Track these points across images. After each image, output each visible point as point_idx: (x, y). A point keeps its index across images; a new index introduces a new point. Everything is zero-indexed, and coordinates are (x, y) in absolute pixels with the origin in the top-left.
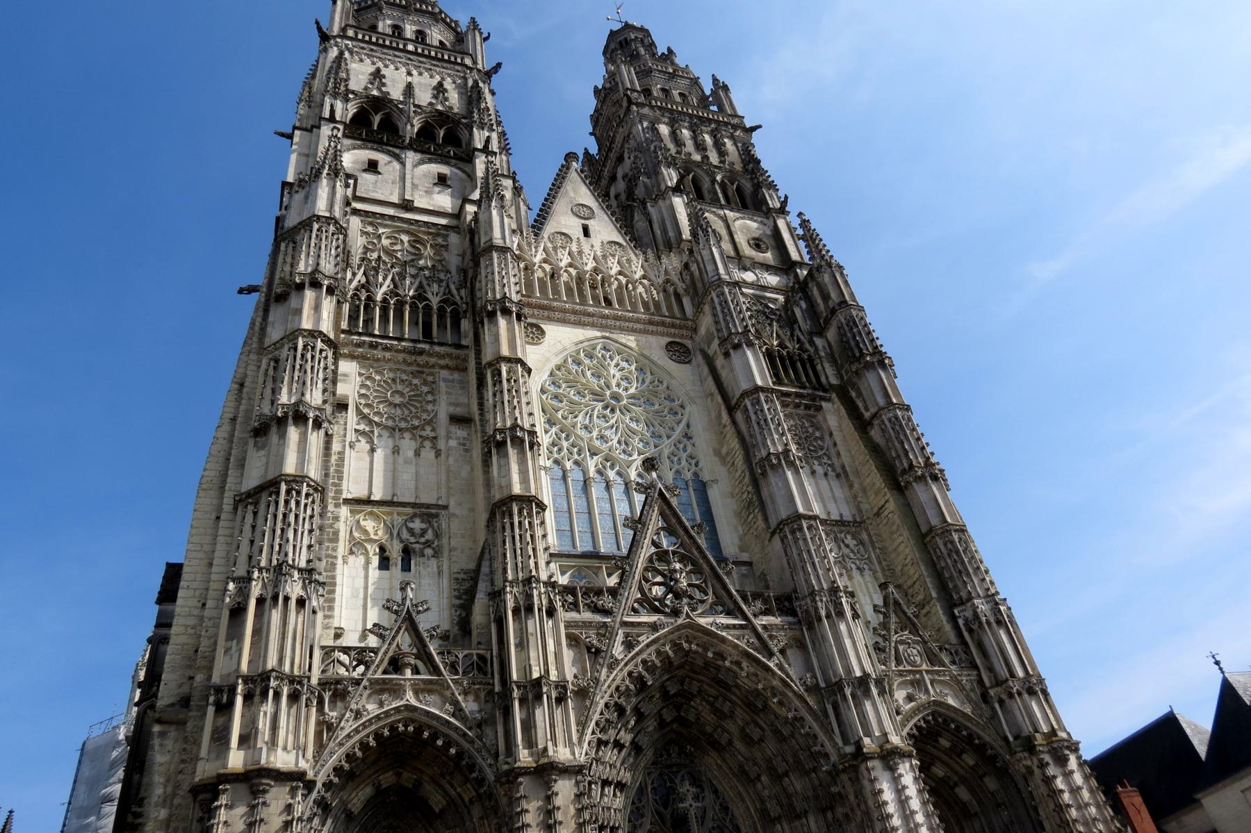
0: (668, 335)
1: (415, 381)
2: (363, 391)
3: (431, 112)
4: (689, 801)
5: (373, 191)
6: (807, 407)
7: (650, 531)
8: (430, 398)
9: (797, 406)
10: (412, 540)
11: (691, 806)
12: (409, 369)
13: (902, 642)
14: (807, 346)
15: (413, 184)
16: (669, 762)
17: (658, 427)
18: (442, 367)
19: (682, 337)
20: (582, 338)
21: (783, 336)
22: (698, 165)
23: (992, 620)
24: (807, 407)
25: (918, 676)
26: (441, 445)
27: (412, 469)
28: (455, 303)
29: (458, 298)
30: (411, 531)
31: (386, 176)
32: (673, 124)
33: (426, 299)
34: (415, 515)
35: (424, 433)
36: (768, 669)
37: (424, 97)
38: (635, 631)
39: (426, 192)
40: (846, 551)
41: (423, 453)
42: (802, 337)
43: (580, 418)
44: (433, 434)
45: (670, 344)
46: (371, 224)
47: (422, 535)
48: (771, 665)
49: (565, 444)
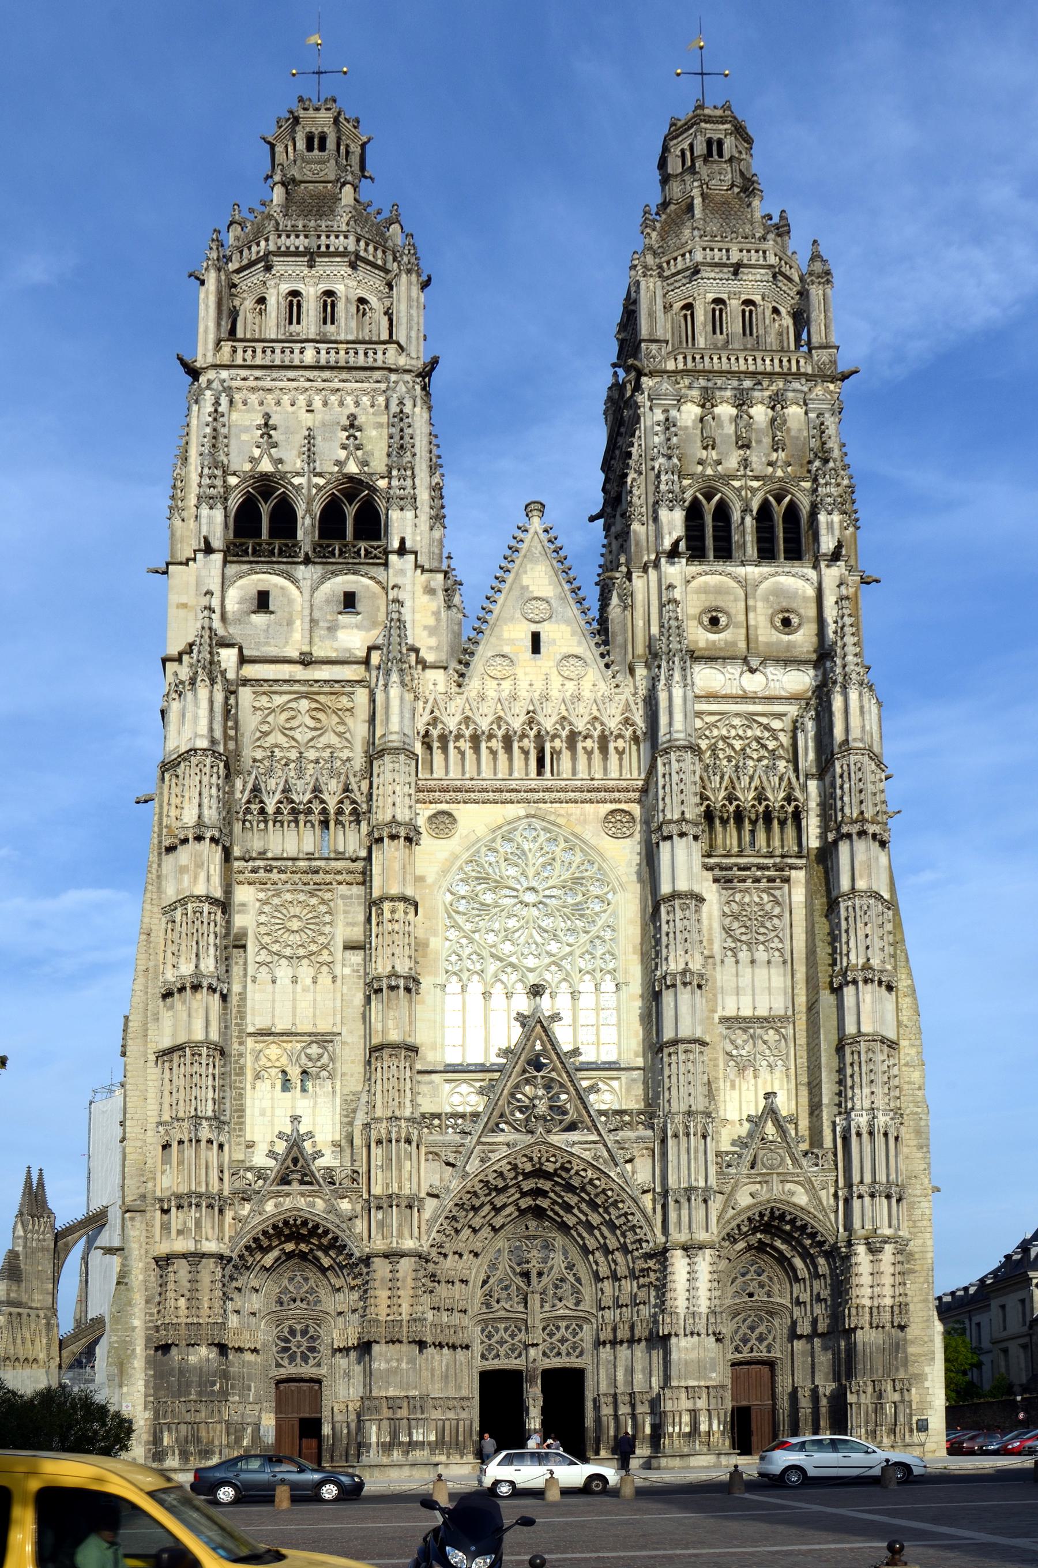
0: (613, 801)
1: (314, 901)
2: (263, 919)
5: (267, 644)
8: (327, 918)
10: (310, 1064)
12: (306, 888)
14: (798, 794)
15: (313, 622)
18: (340, 883)
19: (629, 801)
20: (500, 821)
21: (766, 784)
22: (727, 478)
25: (767, 1178)
26: (338, 970)
27: (310, 996)
28: (354, 802)
29: (358, 794)
30: (309, 1057)
31: (279, 614)
32: (707, 401)
33: (323, 802)
34: (312, 1042)
35: (320, 959)
39: (329, 629)
41: (320, 980)
42: (794, 780)
44: (329, 959)
45: (612, 812)
46: (264, 693)
47: (318, 1060)
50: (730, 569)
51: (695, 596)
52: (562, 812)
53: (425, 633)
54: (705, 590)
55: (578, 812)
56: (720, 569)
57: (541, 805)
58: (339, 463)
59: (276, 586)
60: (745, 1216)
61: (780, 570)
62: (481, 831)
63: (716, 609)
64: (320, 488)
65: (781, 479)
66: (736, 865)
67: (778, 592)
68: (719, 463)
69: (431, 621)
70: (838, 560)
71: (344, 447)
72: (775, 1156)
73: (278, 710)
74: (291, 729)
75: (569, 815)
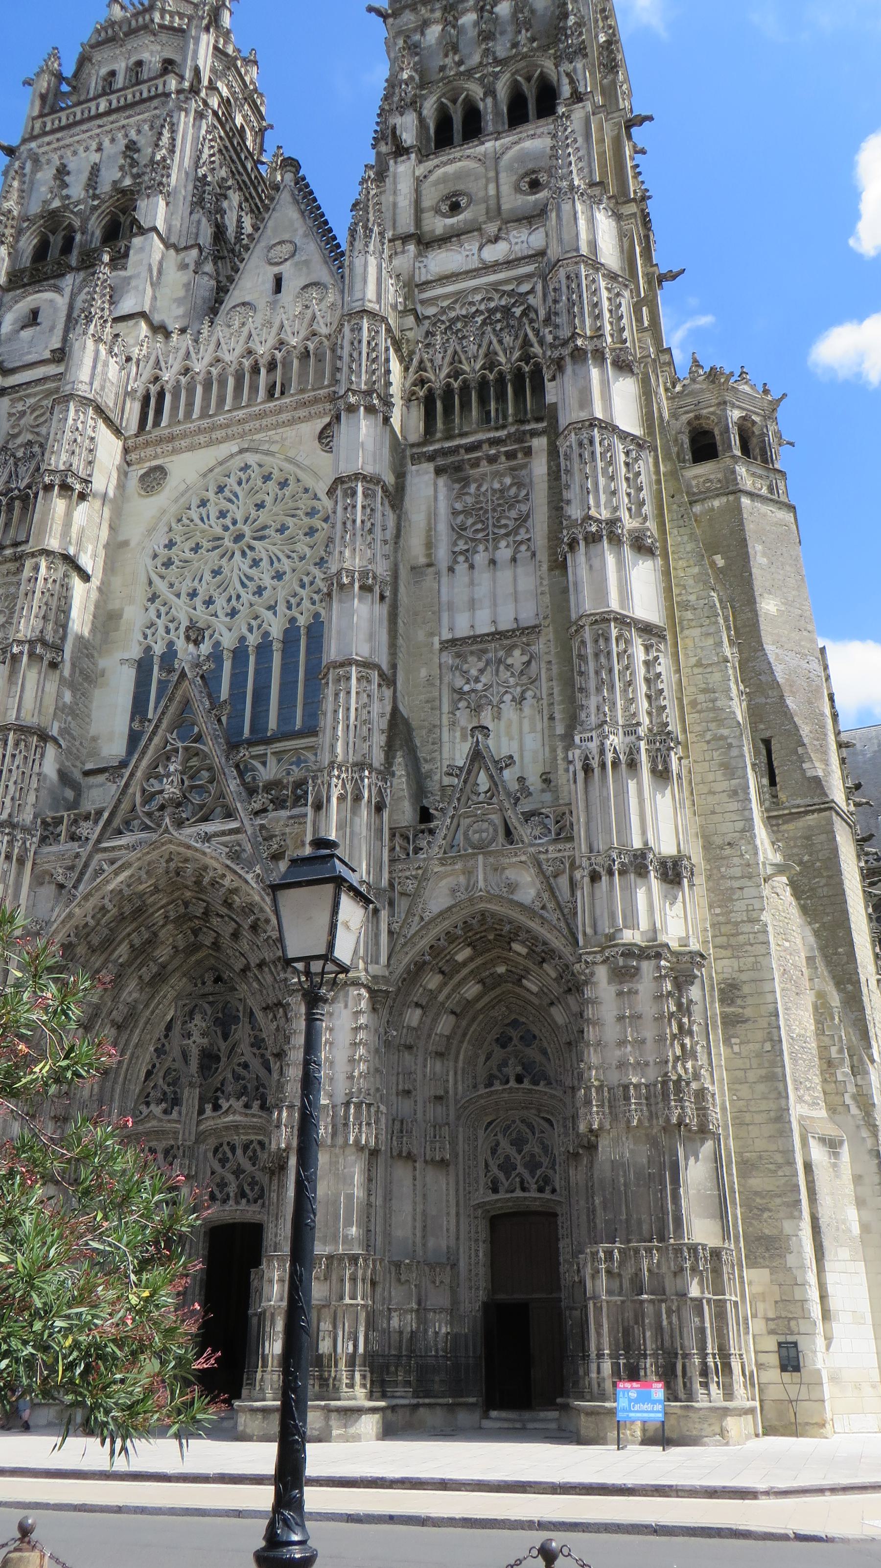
3: (111, 197)
4: (196, 1037)
5: (29, 353)
6: (510, 455)
7: (164, 725)
9: (492, 460)
11: (194, 1042)
13: (466, 815)
14: (537, 349)
16: (202, 992)
17: (284, 560)
20: (212, 463)
21: (496, 346)
22: (469, 74)
23: (595, 764)
24: (510, 455)
36: (247, 882)
37: (110, 175)
38: (112, 855)
40: (504, 674)
43: (188, 581)
46: (21, 399)
48: (249, 877)
49: (160, 623)
50: (468, 152)
51: (433, 189)
52: (277, 438)
53: (175, 305)
54: (445, 179)
55: (294, 432)
56: (458, 155)
57: (255, 437)
58: (115, 183)
59: (46, 300)
60: (435, 931)
61: (524, 135)
62: (192, 477)
63: (456, 194)
64: (94, 208)
65: (525, 57)
66: (458, 447)
67: (522, 158)
68: (460, 63)
69: (181, 293)
70: (580, 100)
71: (121, 168)
72: (485, 825)
73: (29, 411)
74: (38, 426)
75: (283, 439)
